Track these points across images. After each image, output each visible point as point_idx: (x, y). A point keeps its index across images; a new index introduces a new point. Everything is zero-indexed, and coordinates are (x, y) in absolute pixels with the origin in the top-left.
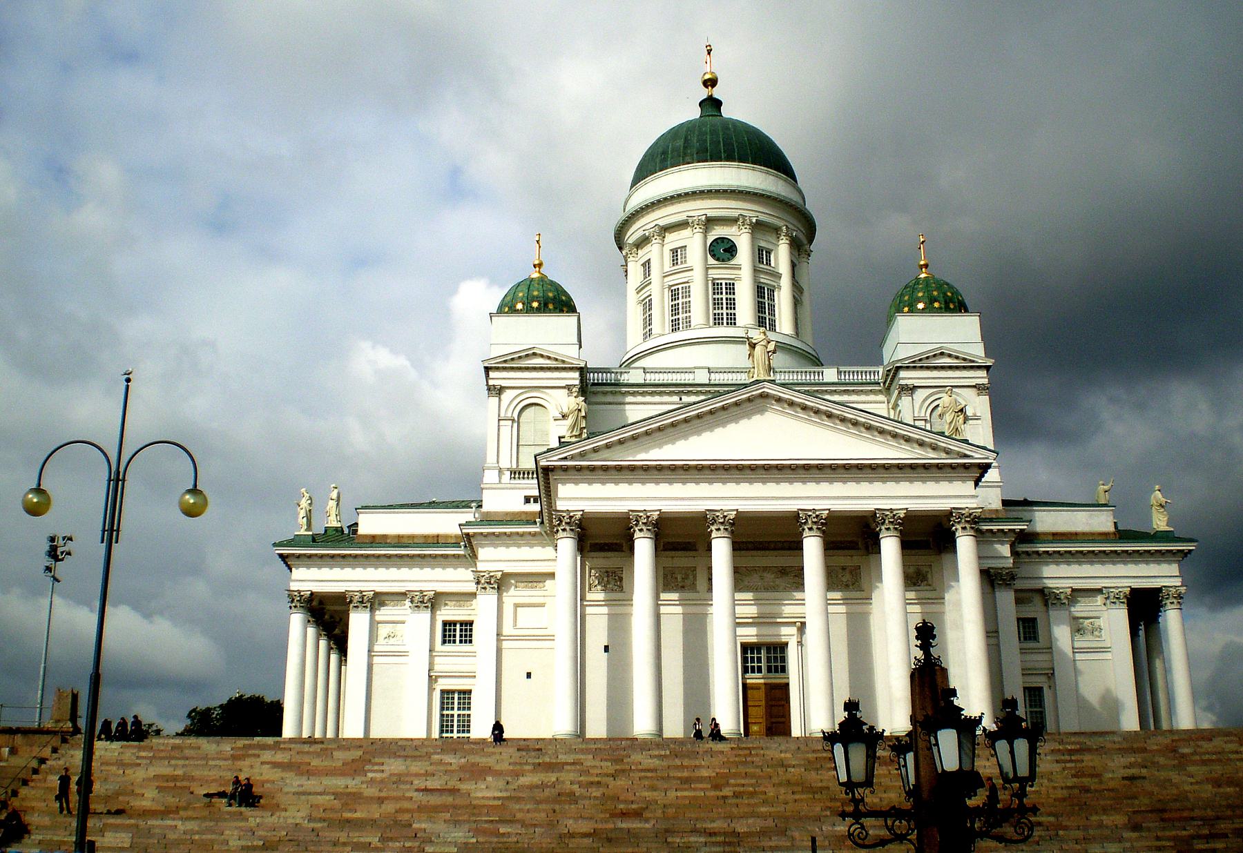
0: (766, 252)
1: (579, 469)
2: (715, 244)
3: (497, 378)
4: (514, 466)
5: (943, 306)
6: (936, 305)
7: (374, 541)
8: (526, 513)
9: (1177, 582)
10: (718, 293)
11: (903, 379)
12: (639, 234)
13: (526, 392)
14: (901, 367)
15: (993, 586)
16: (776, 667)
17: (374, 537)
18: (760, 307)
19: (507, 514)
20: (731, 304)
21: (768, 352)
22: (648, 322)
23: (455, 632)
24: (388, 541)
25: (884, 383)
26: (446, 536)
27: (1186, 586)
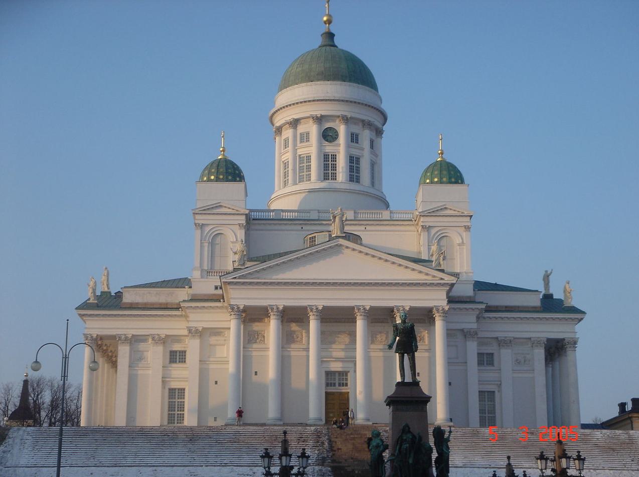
0: (356, 135)
1: (244, 283)
3: (201, 219)
7: (132, 307)
10: (327, 161)
11: (422, 222)
12: (283, 122)
13: (216, 227)
15: (466, 337)
18: (351, 169)
19: (205, 295)
20: (334, 167)
22: (286, 175)
23: (177, 357)
25: (416, 221)
26: (172, 304)
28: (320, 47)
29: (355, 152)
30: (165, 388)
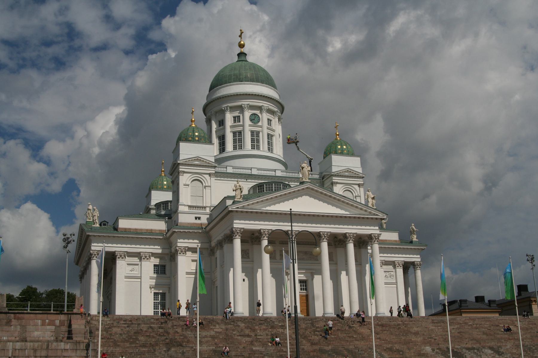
1: (242, 212)
2: (251, 116)
4: (189, 204)
5: (347, 152)
6: (345, 151)
8: (196, 224)
9: (419, 260)
11: (334, 179)
14: (333, 175)
16: (304, 288)
17: (125, 229)
19: (189, 224)
20: (258, 141)
21: (308, 171)
24: (132, 231)
26: (155, 230)
27: (422, 261)
28: (237, 61)
29: (271, 132)
30: (151, 292)
